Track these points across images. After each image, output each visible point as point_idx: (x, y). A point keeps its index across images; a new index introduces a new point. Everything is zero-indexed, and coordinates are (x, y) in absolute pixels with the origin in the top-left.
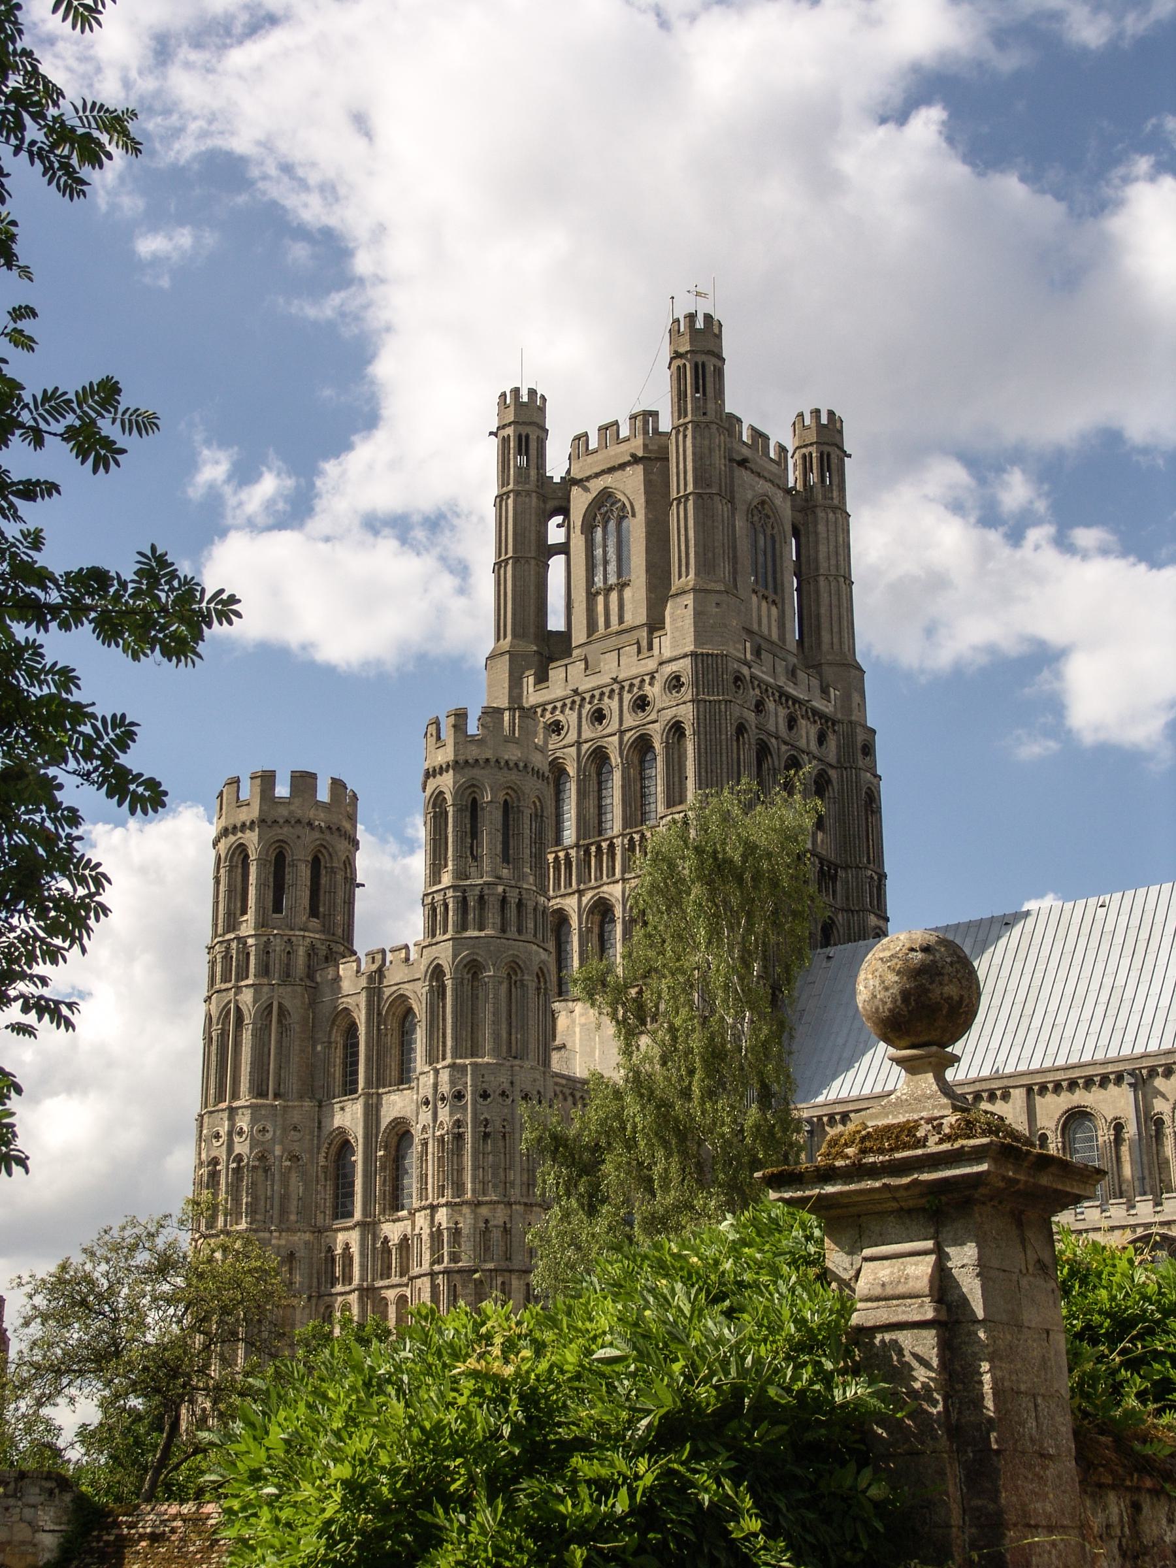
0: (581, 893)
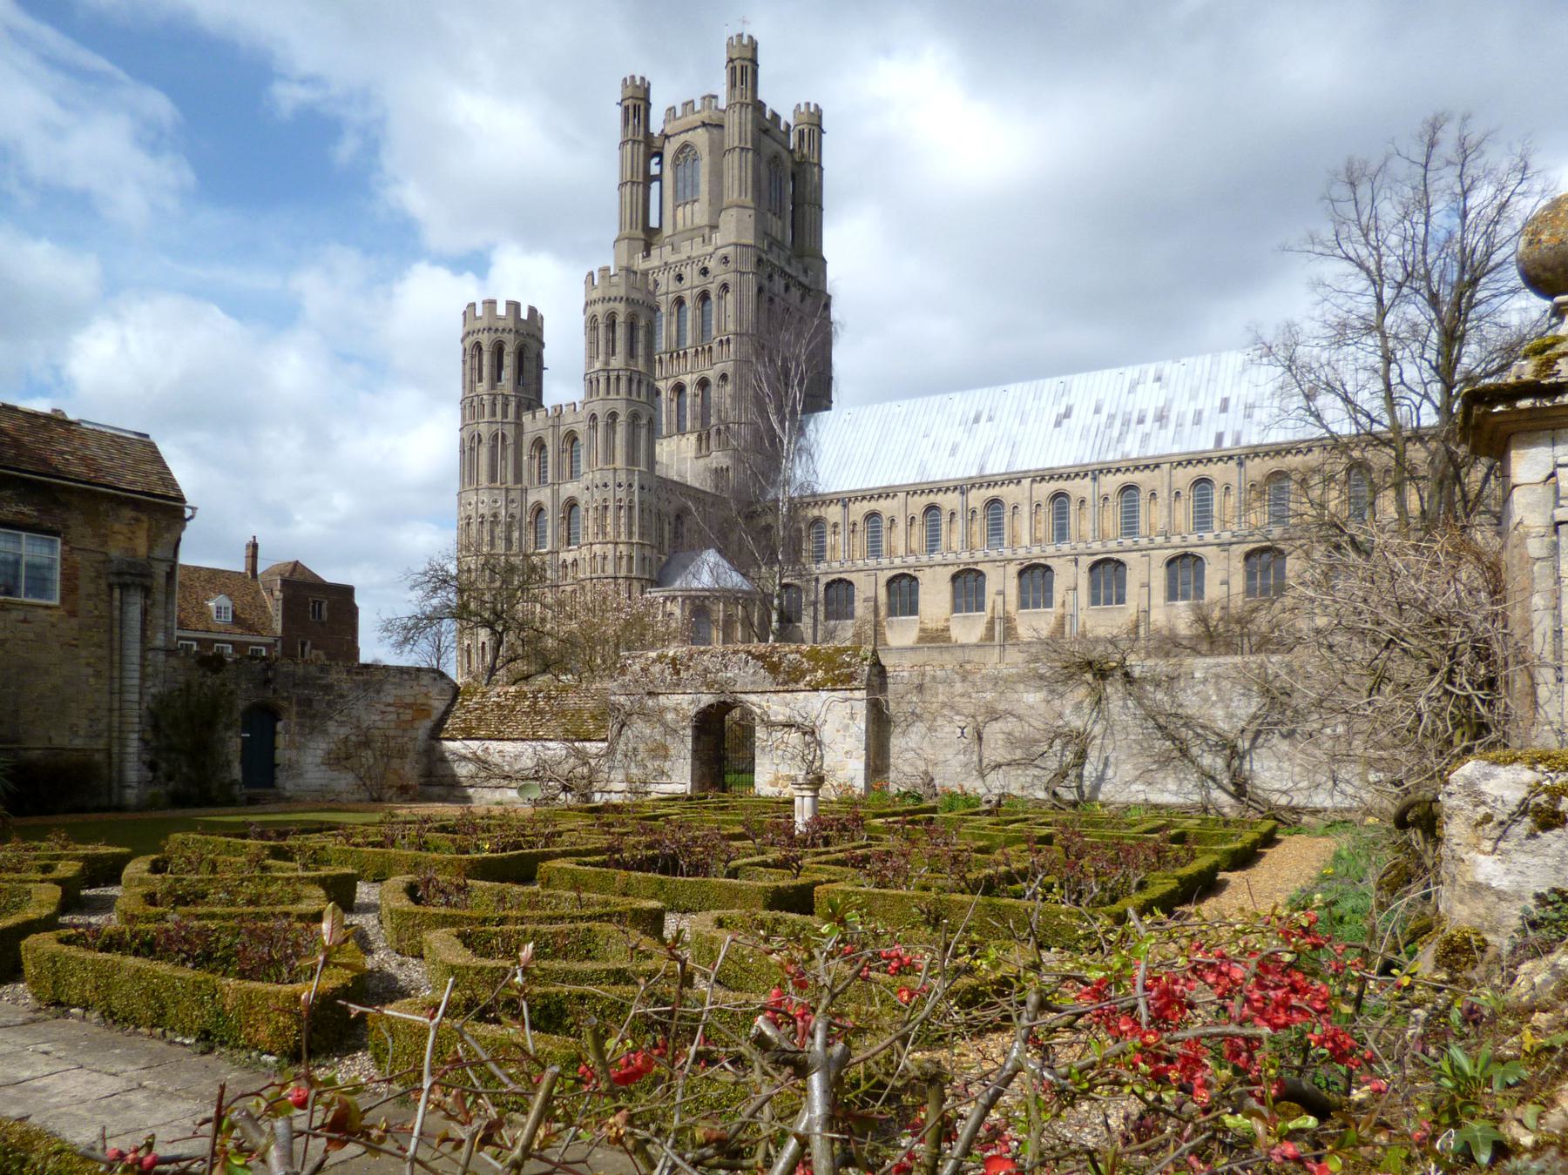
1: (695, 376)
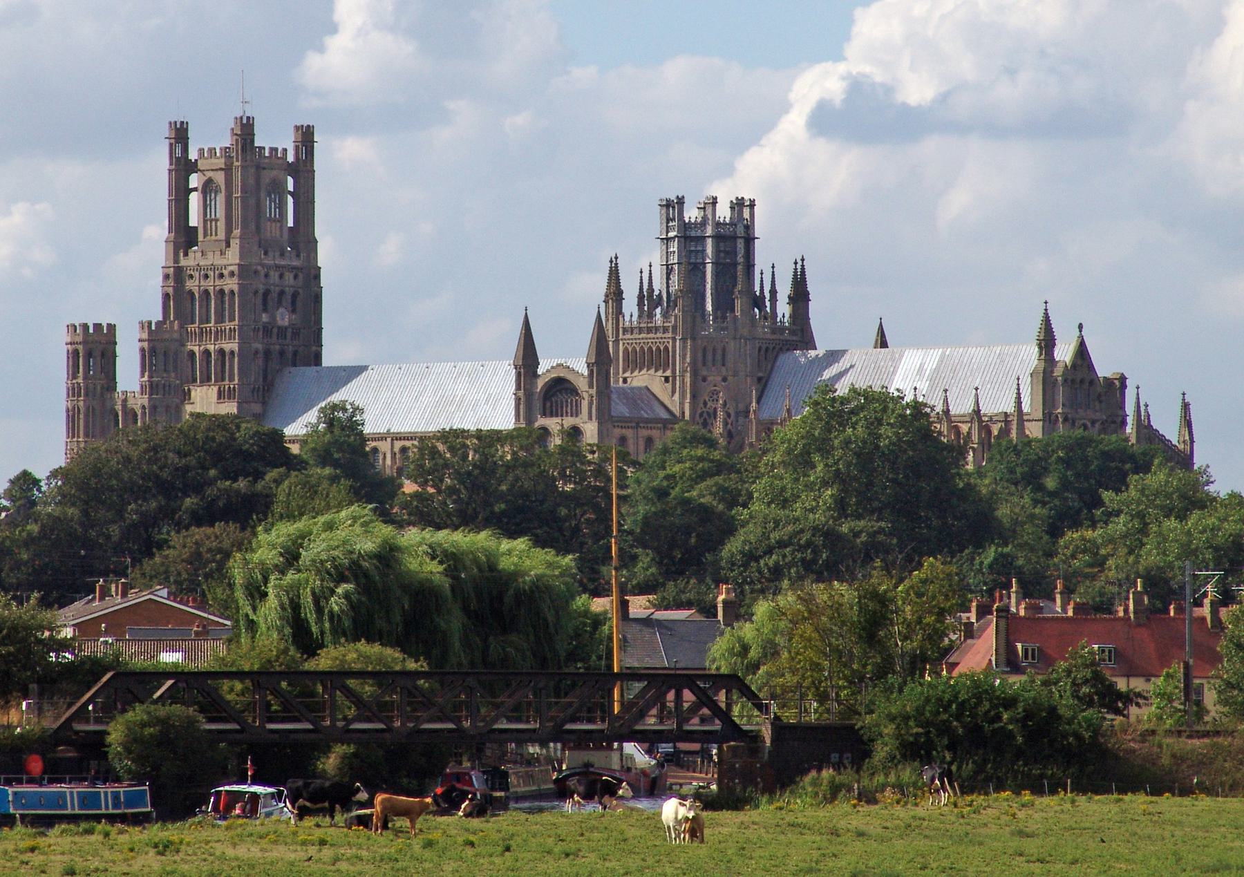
0: (200, 346)
1: (217, 347)
